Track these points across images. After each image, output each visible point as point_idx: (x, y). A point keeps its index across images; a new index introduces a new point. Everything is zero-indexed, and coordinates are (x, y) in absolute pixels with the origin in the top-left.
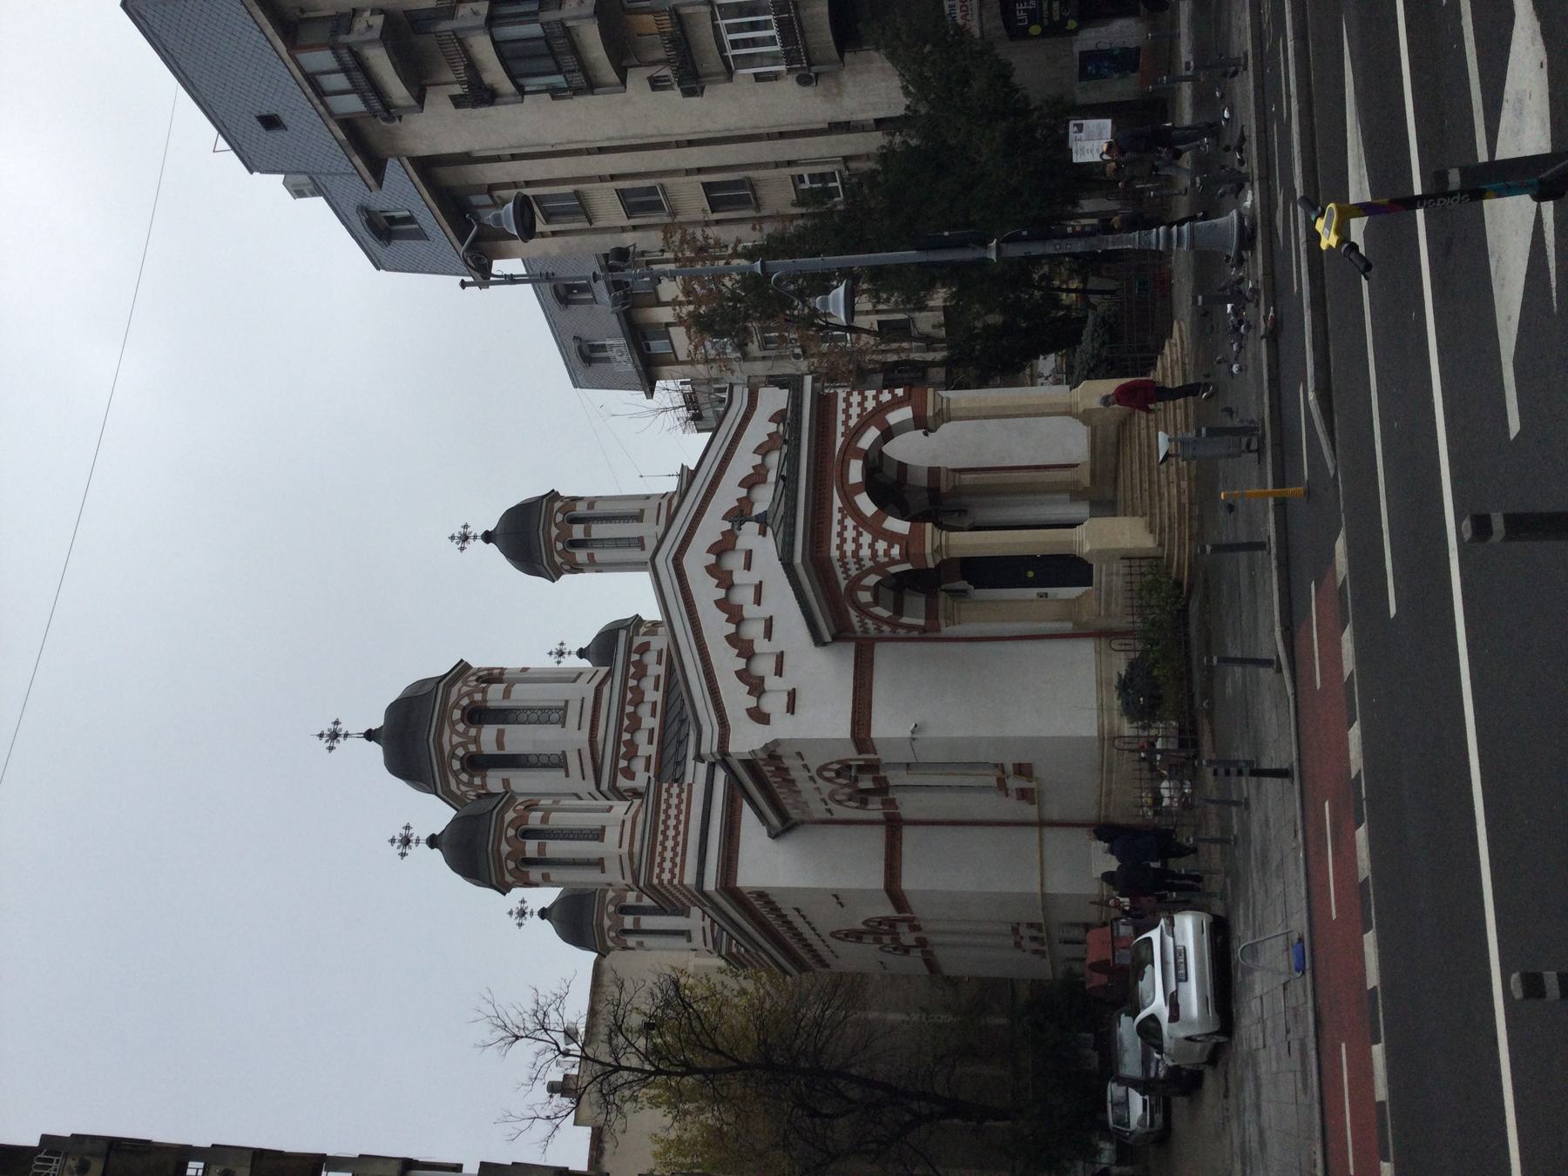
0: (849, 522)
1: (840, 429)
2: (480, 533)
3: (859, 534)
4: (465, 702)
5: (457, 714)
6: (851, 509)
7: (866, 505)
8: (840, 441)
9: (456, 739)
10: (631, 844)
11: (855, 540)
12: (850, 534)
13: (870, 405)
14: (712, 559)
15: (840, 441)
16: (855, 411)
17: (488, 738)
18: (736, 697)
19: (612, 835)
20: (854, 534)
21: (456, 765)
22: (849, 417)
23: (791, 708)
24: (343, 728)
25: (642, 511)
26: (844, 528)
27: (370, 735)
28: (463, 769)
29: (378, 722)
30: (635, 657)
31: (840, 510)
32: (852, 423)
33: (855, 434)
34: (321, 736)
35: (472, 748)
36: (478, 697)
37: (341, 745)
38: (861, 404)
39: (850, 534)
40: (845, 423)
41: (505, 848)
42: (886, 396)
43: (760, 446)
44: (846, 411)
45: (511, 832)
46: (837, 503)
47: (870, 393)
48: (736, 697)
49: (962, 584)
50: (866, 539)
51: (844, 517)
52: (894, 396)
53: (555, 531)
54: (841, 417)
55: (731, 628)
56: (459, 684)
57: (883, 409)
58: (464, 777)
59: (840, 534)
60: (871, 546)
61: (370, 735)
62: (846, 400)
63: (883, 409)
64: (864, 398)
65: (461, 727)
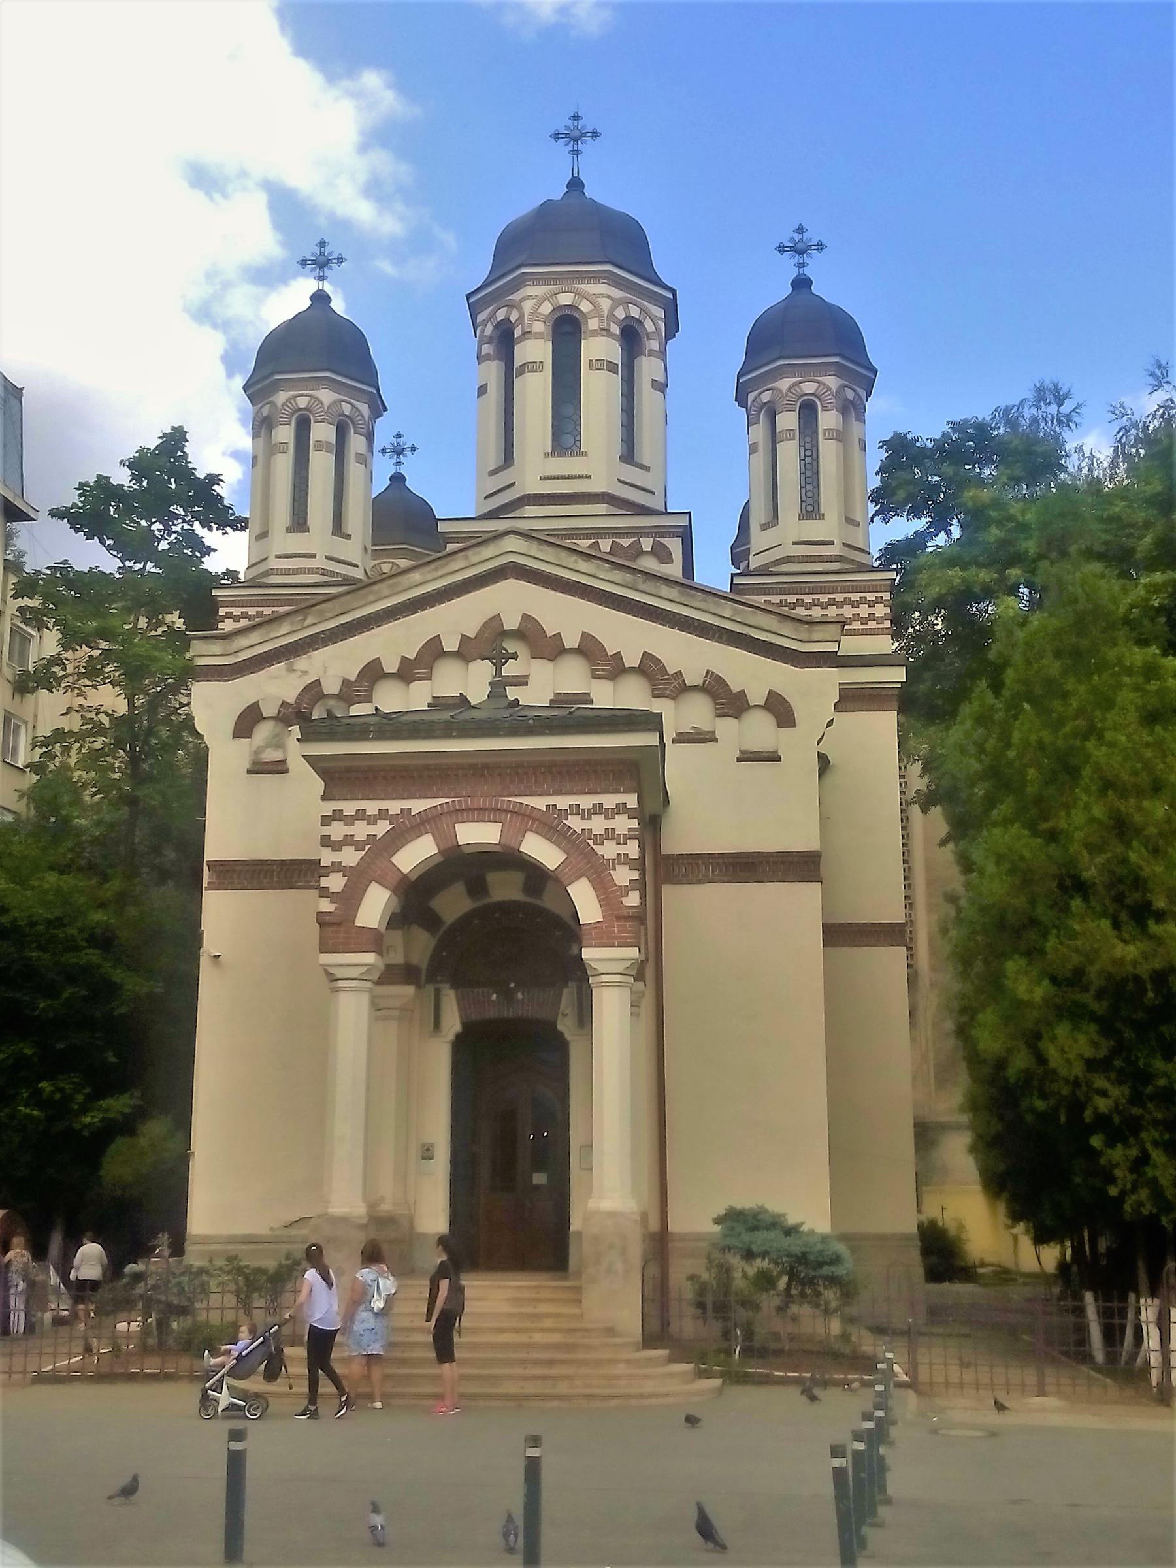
0: (382, 828)
1: (563, 802)
2: (808, 271)
3: (359, 846)
4: (585, 307)
5: (566, 299)
6: (405, 830)
7: (416, 854)
8: (539, 803)
9: (528, 306)
10: (287, 572)
11: (348, 841)
12: (361, 830)
13: (609, 850)
14: (512, 622)
15: (539, 803)
16: (598, 825)
17: (536, 350)
18: (277, 686)
19: (297, 542)
20: (360, 836)
21: (501, 315)
22: (586, 815)
23: (259, 768)
24: (588, 147)
25: (822, 517)
26: (372, 820)
27: (576, 185)
28: (498, 326)
29: (591, 192)
30: (647, 544)
31: (406, 812)
32: (575, 823)
33: (551, 826)
34: (576, 117)
35: (517, 333)
36: (593, 324)
37: (562, 148)
38: (610, 835)
39: (361, 830)
40: (575, 810)
41: (281, 397)
42: (623, 876)
43: (719, 680)
44: (597, 809)
45: (302, 402)
46: (418, 806)
47: (632, 849)
48: (277, 686)
49: (453, 1024)
50: (350, 857)
51: (392, 818)
52: (626, 891)
53: (784, 384)
54: (586, 802)
55: (390, 666)
56: (618, 294)
57: (599, 873)
58: (489, 329)
59: (361, 815)
60: (336, 867)
61: (576, 185)
62: (621, 809)
63: (599, 873)
64: (623, 840)
65: (546, 308)
